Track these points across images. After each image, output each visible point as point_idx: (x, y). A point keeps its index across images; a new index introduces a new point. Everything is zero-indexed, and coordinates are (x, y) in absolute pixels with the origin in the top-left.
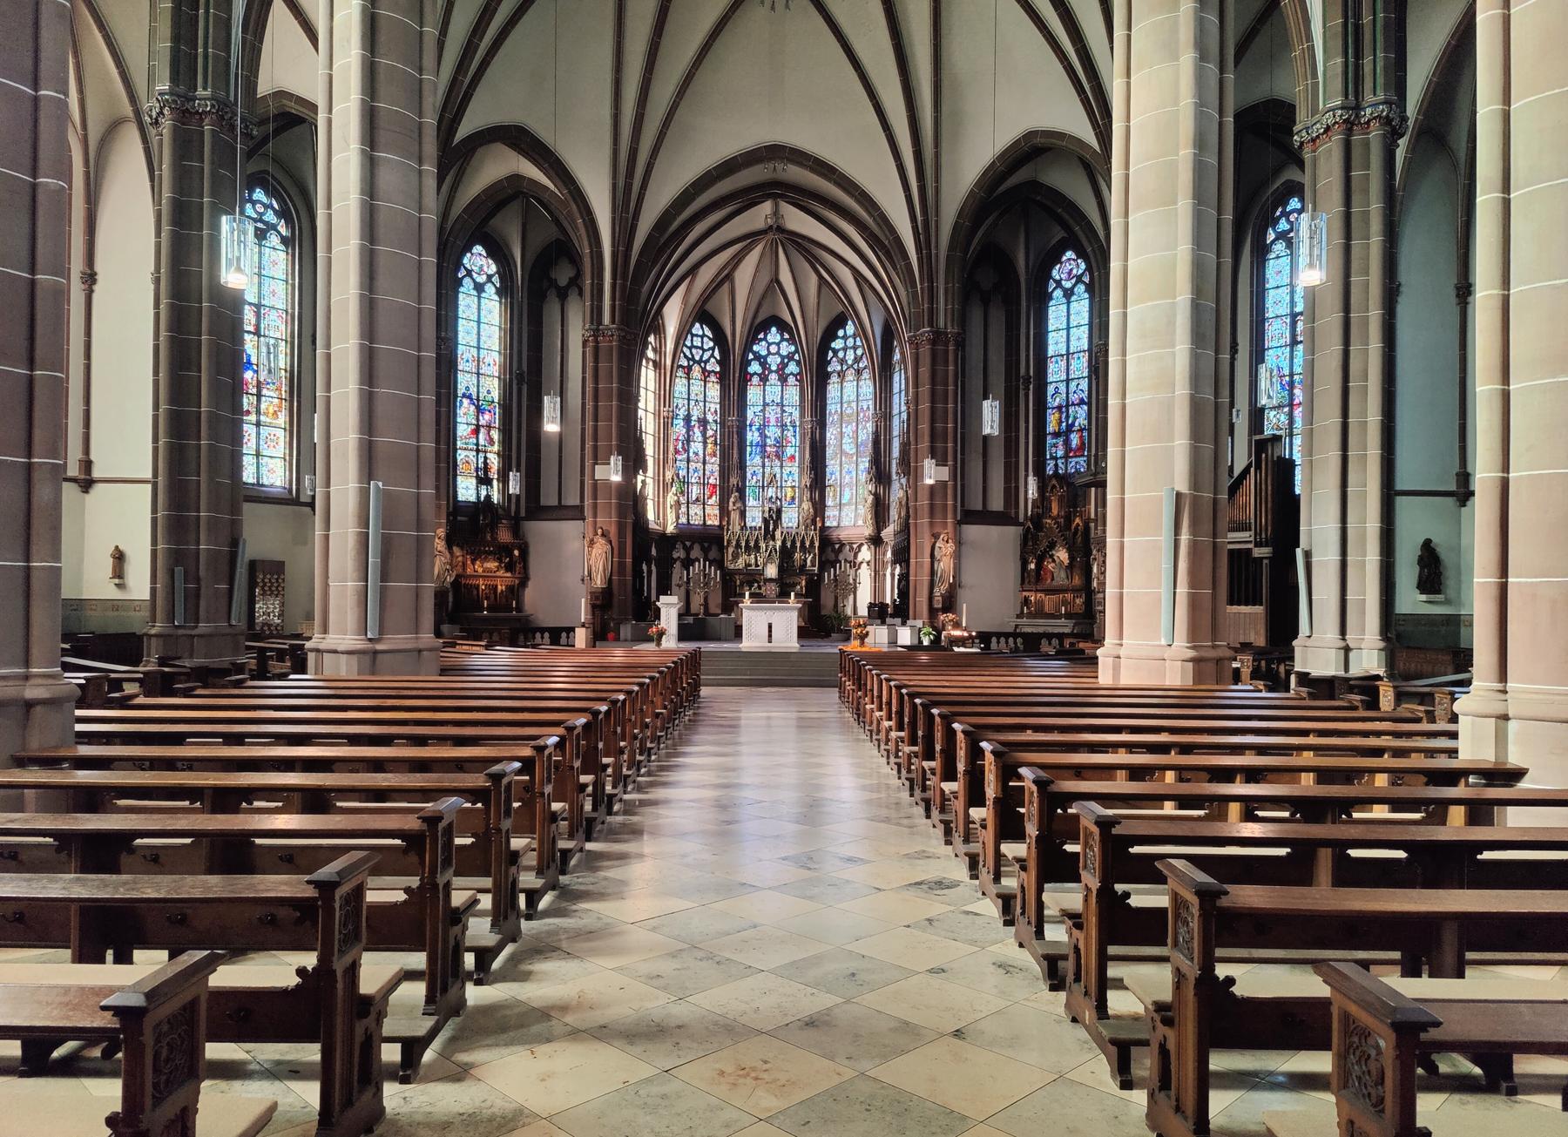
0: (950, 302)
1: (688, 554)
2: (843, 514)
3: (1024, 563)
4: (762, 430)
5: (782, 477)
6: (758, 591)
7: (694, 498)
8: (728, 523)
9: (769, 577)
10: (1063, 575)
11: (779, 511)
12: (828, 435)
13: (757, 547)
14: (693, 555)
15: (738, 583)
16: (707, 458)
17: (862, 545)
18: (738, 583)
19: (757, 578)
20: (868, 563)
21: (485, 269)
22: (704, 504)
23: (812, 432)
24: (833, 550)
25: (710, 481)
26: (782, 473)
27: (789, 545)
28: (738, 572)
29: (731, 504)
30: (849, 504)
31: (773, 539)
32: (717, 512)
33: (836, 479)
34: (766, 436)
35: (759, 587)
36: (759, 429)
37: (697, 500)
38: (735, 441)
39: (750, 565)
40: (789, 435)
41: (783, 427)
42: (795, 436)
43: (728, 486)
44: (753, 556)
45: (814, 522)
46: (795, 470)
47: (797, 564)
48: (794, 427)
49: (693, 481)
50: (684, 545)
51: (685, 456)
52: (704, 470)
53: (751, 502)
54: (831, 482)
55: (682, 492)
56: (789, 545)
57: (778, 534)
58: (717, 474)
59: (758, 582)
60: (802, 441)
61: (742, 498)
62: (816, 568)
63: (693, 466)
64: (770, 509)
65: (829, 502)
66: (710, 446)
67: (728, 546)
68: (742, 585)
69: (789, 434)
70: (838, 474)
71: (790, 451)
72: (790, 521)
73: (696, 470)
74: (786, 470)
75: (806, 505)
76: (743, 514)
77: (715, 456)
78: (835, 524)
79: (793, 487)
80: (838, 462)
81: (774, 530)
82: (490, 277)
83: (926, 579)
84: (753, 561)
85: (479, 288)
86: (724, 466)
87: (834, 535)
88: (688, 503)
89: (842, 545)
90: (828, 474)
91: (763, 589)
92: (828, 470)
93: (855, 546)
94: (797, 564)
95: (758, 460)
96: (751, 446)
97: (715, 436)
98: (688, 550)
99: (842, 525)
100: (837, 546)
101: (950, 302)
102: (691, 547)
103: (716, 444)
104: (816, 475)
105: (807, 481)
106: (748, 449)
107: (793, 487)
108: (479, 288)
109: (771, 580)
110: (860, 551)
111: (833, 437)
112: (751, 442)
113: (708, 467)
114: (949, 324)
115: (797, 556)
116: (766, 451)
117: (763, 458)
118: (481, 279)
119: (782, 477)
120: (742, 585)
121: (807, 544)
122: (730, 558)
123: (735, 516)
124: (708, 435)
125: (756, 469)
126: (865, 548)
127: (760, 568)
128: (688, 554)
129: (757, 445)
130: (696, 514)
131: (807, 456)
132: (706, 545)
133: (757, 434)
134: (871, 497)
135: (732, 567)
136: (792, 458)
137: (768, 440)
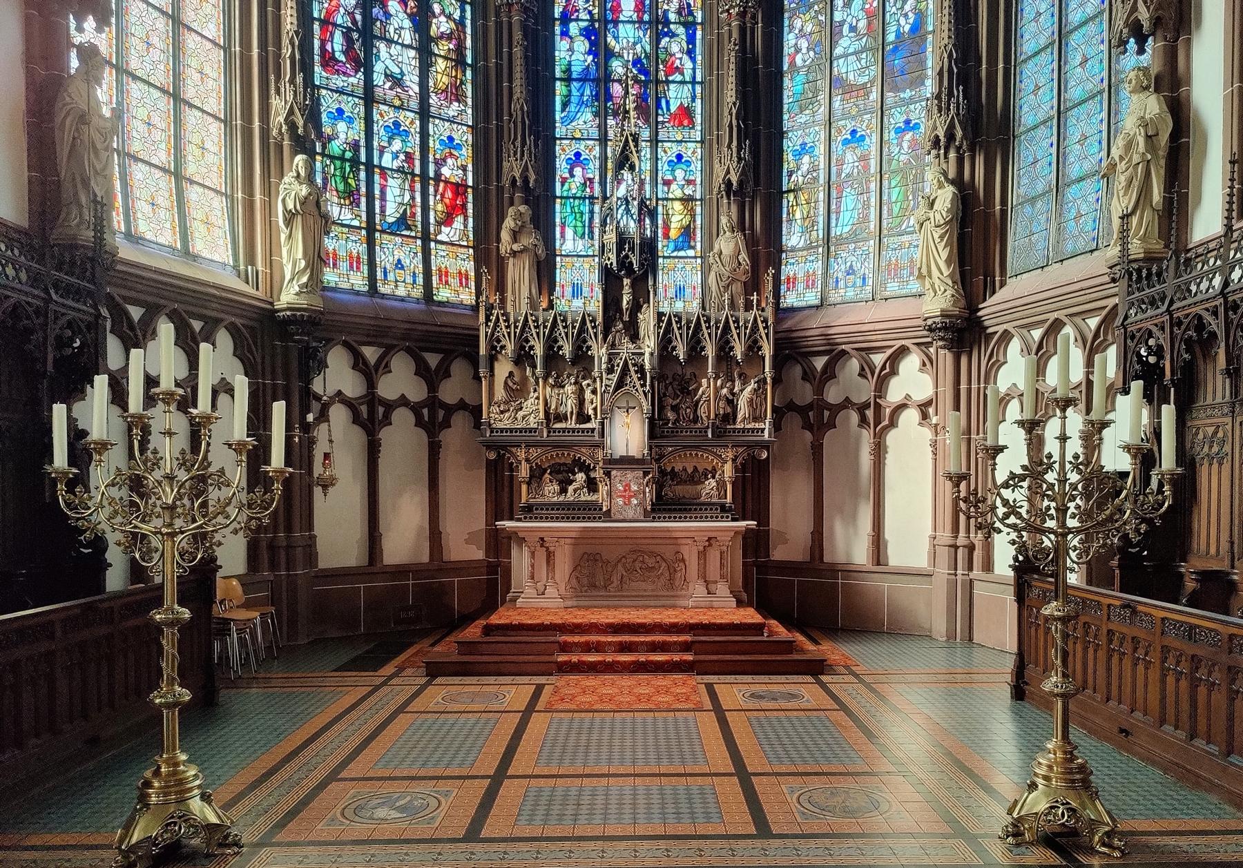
1: (371, 385)
2: (838, 269)
4: (595, 36)
5: (655, 171)
6: (585, 497)
7: (392, 212)
8: (503, 301)
9: (620, 451)
11: (649, 248)
12: (790, 40)
13: (582, 359)
14: (388, 388)
15: (524, 472)
16: (433, 100)
17: (903, 351)
18: (524, 472)
19: (584, 455)
20: (924, 408)
22: (426, 238)
23: (742, 30)
24: (808, 375)
25: (446, 171)
26: (655, 159)
27: (681, 352)
28: (527, 438)
29: (505, 236)
30: (854, 237)
31: (635, 337)
32: (469, 266)
33: (814, 169)
34: (610, 54)
35: (592, 485)
36: (587, 33)
37: (403, 222)
38: (517, 51)
39: (561, 418)
40: (675, 48)
41: (657, 26)
42: (690, 53)
43: (500, 190)
44: (569, 389)
45: (753, 285)
46: (692, 151)
47: (708, 411)
48: (689, 26)
49: (387, 161)
50: (359, 363)
51: (357, 80)
52: (424, 135)
53: (569, 242)
54: (798, 178)
55: (350, 196)
56: (681, 352)
57: (647, 320)
58: (466, 154)
59: (586, 469)
60: (713, 63)
61: (542, 221)
62: (767, 425)
63: (384, 116)
64: (622, 240)
65: (793, 238)
66: (441, 64)
67: (492, 359)
68: (536, 475)
69: (676, 47)
70: (821, 149)
71: (677, 96)
72: (680, 291)
73: (396, 130)
74: (668, 151)
75: (727, 244)
76: (545, 272)
77: (458, 97)
78: (812, 298)
79: (687, 200)
80: (822, 111)
81: (636, 308)
84: (570, 405)
86: (487, 131)
87: (814, 325)
88: (371, 228)
89: (837, 356)
90: (789, 157)
91: (603, 489)
92: (790, 145)
93: (878, 359)
94: (708, 411)
95: (585, 120)
96: (568, 80)
97: (456, 36)
98: (369, 373)
99: (834, 297)
100: (820, 363)
102: (383, 365)
103: (460, 62)
104: (755, 152)
105: (728, 167)
106: (560, 88)
107: (687, 200)
109: (627, 462)
110: (894, 372)
111: (804, 44)
112: (568, 70)
113: (439, 130)
115: (708, 387)
116: (609, 97)
117: (601, 115)
119: (655, 171)
120: (536, 475)
121: (739, 351)
122: (500, 393)
123: (520, 275)
124: (434, 31)
125: (581, 147)
126: (911, 364)
127: (593, 424)
128: (371, 385)
129: (583, 79)
130: (399, 265)
131: (730, 95)
132: (433, 360)
133: (582, 45)
134: (949, 191)
135: (505, 422)
136: (685, 114)
137: (617, 67)
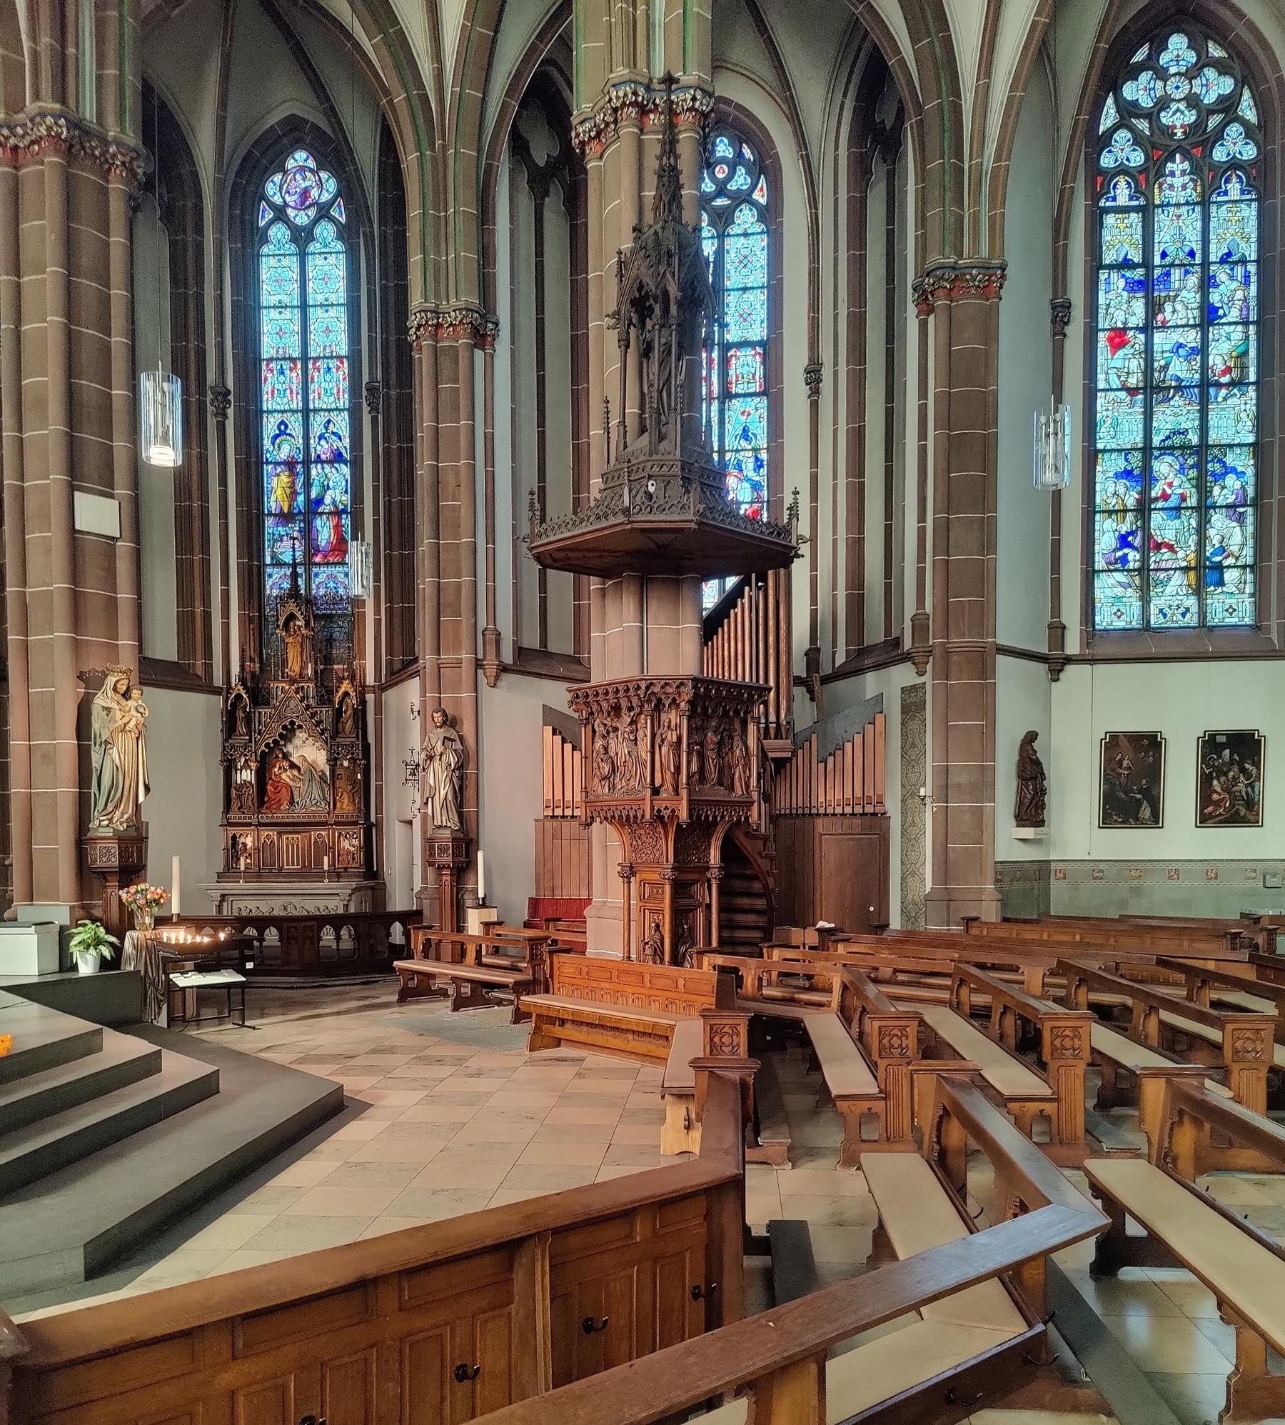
0: (111, 56)
3: (229, 767)
10: (316, 793)
21: (314, 193)
82: (324, 212)
83: (66, 791)
85: (302, 237)
101: (111, 56)
108: (302, 237)
114: (111, 119)
118: (302, 219)
